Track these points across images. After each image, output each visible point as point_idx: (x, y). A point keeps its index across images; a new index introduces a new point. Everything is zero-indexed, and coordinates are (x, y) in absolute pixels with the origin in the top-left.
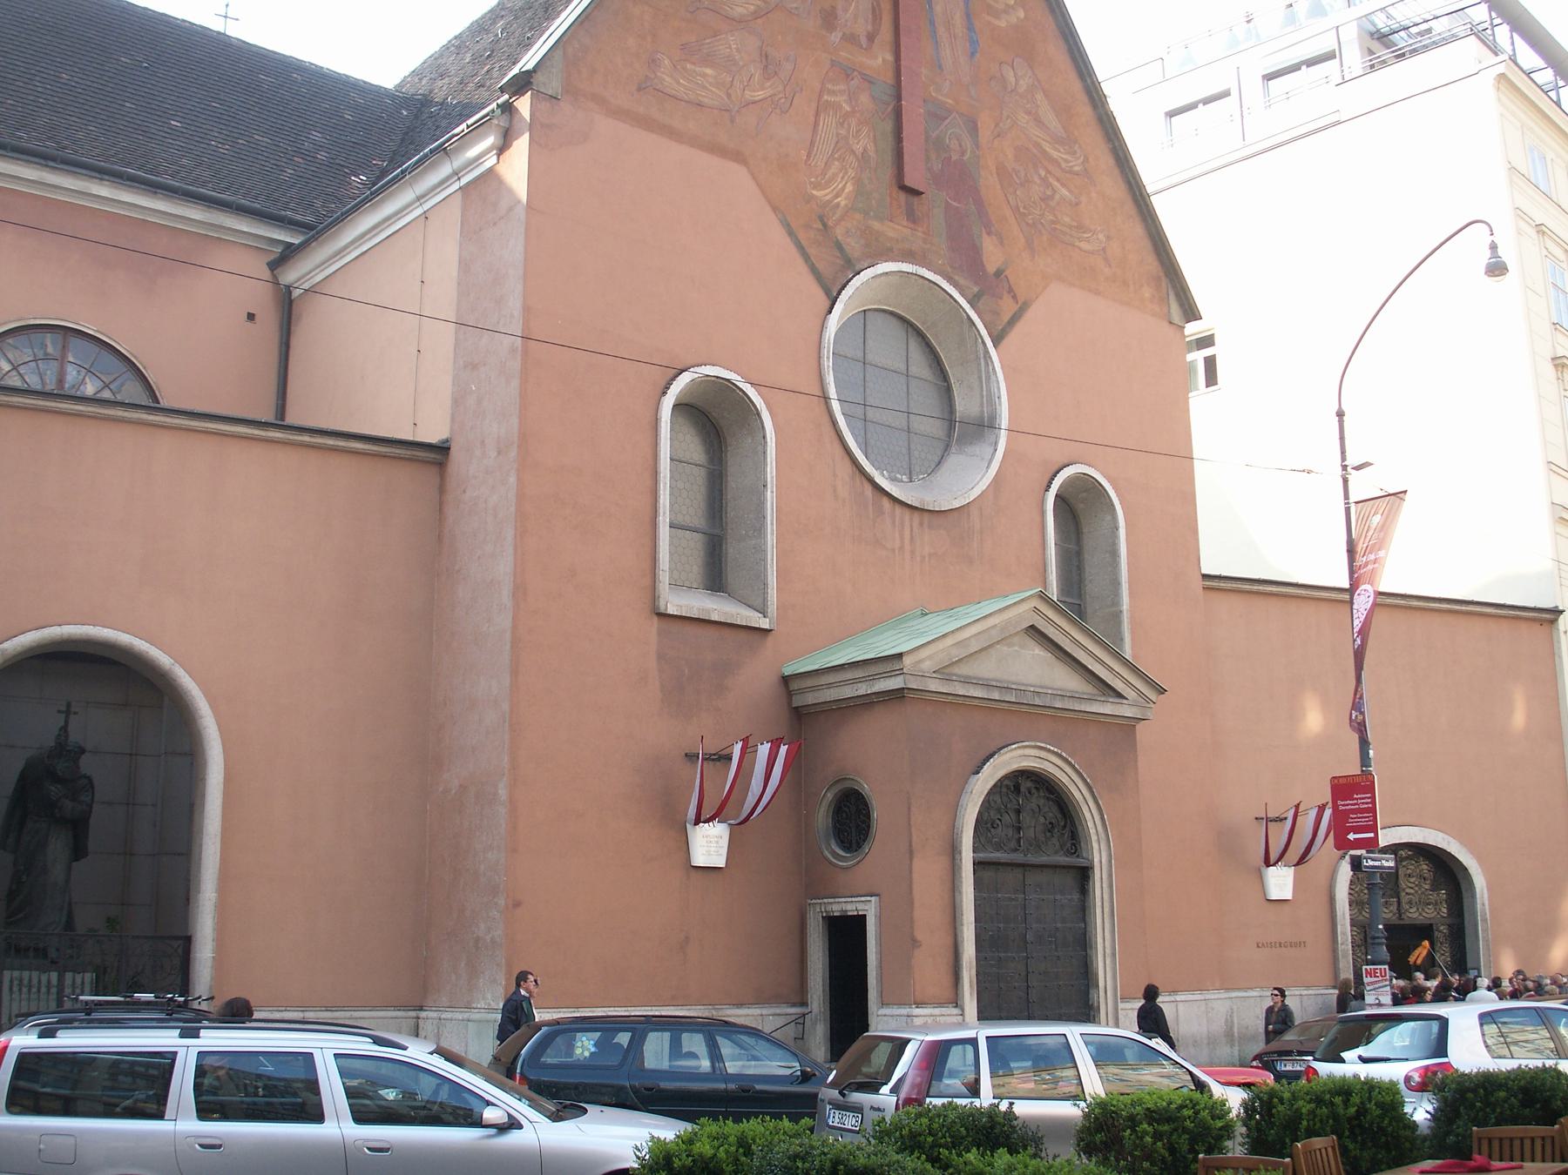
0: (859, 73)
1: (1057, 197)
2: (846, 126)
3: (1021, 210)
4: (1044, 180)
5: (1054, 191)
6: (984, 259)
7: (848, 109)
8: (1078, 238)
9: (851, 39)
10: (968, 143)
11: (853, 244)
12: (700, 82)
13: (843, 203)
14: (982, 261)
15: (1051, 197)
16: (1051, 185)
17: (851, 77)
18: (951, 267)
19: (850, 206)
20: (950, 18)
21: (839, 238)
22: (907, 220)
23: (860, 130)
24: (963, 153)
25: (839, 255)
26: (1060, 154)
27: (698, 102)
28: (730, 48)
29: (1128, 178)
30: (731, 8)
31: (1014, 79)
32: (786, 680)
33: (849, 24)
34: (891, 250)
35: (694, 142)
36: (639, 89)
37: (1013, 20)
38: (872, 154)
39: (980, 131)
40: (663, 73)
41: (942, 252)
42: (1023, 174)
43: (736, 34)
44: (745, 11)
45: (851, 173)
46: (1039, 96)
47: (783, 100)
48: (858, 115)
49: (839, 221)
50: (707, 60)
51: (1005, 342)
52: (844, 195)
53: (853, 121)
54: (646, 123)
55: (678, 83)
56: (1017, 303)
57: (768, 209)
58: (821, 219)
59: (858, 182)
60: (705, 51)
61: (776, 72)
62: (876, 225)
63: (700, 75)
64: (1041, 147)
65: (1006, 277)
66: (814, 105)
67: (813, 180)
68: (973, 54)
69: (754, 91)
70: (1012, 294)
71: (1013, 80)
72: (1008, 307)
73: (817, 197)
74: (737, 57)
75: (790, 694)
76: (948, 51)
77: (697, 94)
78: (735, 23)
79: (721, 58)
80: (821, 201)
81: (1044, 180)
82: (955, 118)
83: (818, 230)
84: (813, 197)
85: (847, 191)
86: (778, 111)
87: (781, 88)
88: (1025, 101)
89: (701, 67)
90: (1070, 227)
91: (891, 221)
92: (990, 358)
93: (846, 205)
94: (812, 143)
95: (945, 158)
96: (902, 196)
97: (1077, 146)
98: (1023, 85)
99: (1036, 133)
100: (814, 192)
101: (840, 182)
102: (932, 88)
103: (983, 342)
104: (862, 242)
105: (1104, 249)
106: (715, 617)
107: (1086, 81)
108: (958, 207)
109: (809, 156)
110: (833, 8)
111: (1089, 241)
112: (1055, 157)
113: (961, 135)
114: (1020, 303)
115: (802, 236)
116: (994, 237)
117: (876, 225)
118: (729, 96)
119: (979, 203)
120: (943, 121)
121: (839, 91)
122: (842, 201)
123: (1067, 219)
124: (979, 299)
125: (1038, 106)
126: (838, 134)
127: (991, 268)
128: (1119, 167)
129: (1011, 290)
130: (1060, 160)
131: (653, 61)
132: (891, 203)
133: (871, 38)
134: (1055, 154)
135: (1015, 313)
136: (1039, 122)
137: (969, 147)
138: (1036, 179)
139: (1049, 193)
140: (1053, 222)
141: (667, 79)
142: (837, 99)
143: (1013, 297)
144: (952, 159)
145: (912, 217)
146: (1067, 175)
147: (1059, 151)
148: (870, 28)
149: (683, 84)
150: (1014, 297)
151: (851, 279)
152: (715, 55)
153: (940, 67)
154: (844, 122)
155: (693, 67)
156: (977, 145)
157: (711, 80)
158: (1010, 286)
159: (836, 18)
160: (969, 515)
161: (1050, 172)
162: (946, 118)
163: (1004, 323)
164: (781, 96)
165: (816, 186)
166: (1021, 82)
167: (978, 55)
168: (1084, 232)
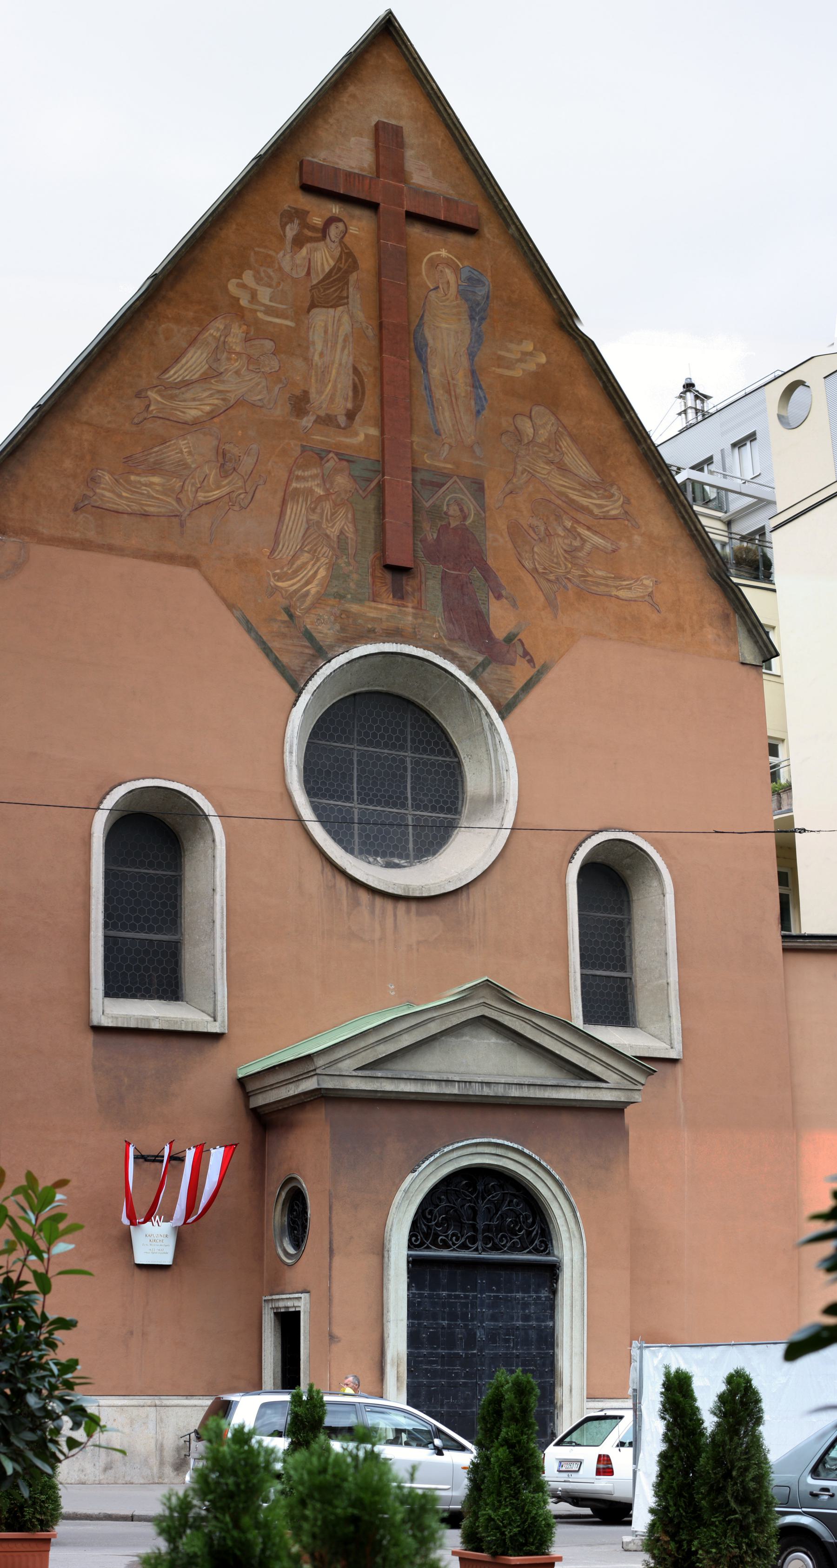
0: (337, 454)
1: (588, 547)
2: (318, 510)
4: (572, 533)
5: (584, 541)
6: (491, 626)
7: (322, 493)
8: (616, 587)
9: (327, 421)
10: (471, 505)
11: (325, 631)
12: (145, 492)
13: (313, 591)
14: (488, 628)
15: (581, 548)
16: (579, 534)
17: (325, 459)
18: (451, 640)
19: (323, 592)
20: (450, 379)
21: (308, 627)
22: (394, 597)
23: (336, 512)
24: (465, 518)
25: (307, 644)
26: (590, 500)
27: (143, 512)
28: (181, 452)
29: (680, 512)
30: (184, 412)
31: (532, 430)
32: (242, 1082)
33: (324, 406)
34: (372, 631)
35: (140, 554)
36: (76, 509)
37: (532, 367)
38: (350, 535)
39: (487, 492)
40: (103, 489)
41: (437, 625)
42: (542, 529)
43: (189, 437)
44: (200, 413)
46: (566, 443)
47: (242, 496)
48: (333, 497)
49: (308, 610)
50: (155, 469)
51: (517, 712)
52: (316, 582)
53: (327, 506)
55: (120, 496)
56: (534, 667)
57: (223, 608)
58: (289, 612)
59: (333, 567)
60: (152, 460)
61: (234, 469)
62: (355, 608)
63: (145, 485)
64: (567, 497)
65: (520, 640)
66: (280, 495)
67: (278, 571)
68: (478, 412)
69: (208, 492)
70: (528, 658)
71: (530, 431)
72: (521, 672)
73: (282, 588)
74: (188, 461)
75: (247, 1096)
76: (447, 414)
77: (143, 504)
78: (186, 426)
79: (170, 464)
80: (286, 591)
81: (572, 533)
82: (455, 482)
83: (284, 622)
84: (277, 588)
85: (319, 576)
86: (237, 508)
87: (240, 483)
88: (546, 451)
89: (146, 477)
90: (605, 578)
91: (374, 601)
92: (496, 729)
93: (318, 592)
94: (277, 534)
95: (441, 526)
96: (388, 576)
97: (615, 487)
98: (544, 434)
99: (561, 482)
100: (279, 584)
101: (311, 569)
102: (426, 455)
103: (487, 714)
104: (337, 627)
105: (650, 595)
106: (156, 1025)
107: (624, 417)
108: (457, 576)
109: (273, 551)
110: (306, 393)
111: (630, 589)
112: (585, 504)
113: (462, 499)
114: (538, 667)
115: (263, 632)
116: (505, 600)
117: (355, 608)
118: (179, 500)
120: (440, 488)
121: (311, 476)
122: (313, 588)
124: (484, 669)
125: (563, 453)
126: (308, 521)
127: (499, 633)
128: (671, 502)
129: (526, 653)
130: (591, 507)
131: (93, 479)
132: (374, 582)
133: (351, 416)
134: (584, 501)
135: (531, 678)
136: (563, 469)
137: (472, 507)
138: (560, 532)
139: (577, 543)
141: (107, 494)
142: (308, 484)
144: (451, 527)
145: (399, 594)
146: (602, 521)
147: (591, 497)
148: (350, 405)
149: (127, 498)
150: (531, 661)
151: (321, 668)
152: (161, 463)
153: (438, 433)
154: (315, 508)
155: (138, 478)
156: (483, 507)
157: (158, 488)
158: (525, 650)
159: (308, 402)
160: (468, 898)
161: (578, 522)
162: (444, 485)
163: (516, 691)
164: (241, 491)
165: (280, 578)
166: (541, 431)
167: (485, 413)
168: (624, 580)
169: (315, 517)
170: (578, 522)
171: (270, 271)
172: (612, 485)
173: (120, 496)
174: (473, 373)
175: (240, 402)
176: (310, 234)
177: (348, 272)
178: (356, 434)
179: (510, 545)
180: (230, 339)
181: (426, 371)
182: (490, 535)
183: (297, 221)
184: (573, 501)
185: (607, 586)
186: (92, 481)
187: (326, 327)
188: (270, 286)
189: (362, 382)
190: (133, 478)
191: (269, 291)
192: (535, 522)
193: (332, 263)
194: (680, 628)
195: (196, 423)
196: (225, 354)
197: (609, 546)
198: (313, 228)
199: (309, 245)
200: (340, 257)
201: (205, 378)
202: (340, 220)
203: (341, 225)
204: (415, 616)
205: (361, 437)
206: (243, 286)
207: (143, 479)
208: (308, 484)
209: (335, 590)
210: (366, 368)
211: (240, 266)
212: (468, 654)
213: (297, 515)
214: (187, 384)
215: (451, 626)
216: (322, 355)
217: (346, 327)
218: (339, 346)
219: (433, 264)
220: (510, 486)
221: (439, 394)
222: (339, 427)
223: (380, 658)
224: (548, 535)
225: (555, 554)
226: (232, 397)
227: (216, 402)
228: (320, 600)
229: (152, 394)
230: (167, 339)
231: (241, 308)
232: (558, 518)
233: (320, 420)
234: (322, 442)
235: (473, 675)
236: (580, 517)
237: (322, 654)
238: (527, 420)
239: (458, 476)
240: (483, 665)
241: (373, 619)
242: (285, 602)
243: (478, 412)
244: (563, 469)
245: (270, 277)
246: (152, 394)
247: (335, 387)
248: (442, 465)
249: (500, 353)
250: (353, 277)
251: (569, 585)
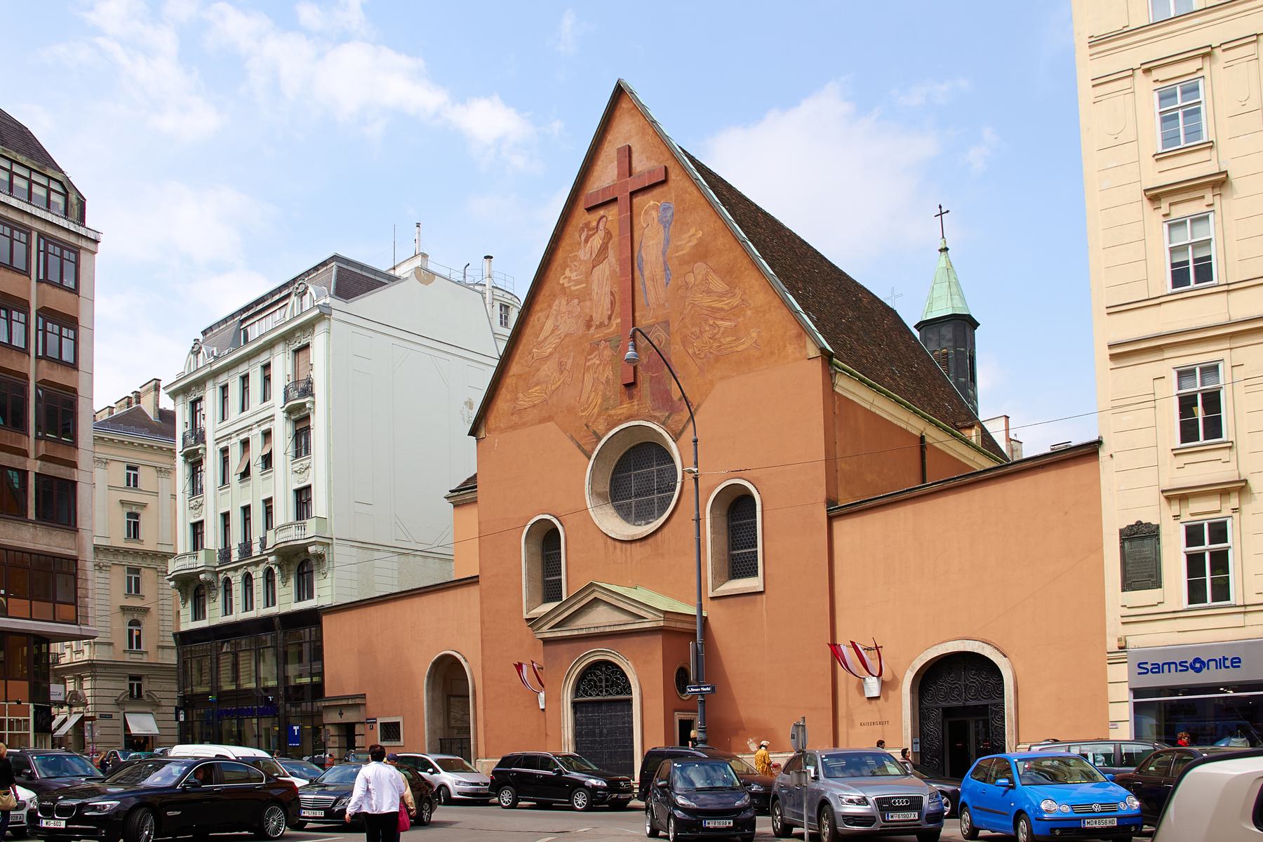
3: (697, 352)
4: (714, 326)
5: (719, 327)
9: (601, 325)
10: (663, 335)
34: (620, 420)
37: (694, 242)
45: (600, 393)
49: (594, 422)
54: (514, 427)
59: (604, 395)
62: (612, 412)
68: (667, 283)
76: (652, 293)
90: (730, 343)
91: (621, 405)
104: (606, 424)
110: (591, 316)
117: (612, 412)
122: (596, 410)
123: (728, 339)
130: (724, 306)
133: (610, 318)
134: (720, 305)
136: (709, 292)
140: (720, 346)
141: (521, 402)
145: (631, 397)
147: (724, 301)
148: (609, 313)
153: (648, 305)
165: (583, 411)
169: (596, 376)
170: (716, 318)
171: (576, 263)
172: (735, 289)
173: (525, 402)
174: (665, 262)
175: (566, 336)
176: (591, 233)
177: (608, 243)
178: (612, 325)
179: (682, 348)
180: (561, 307)
181: (642, 275)
182: (672, 347)
183: (586, 230)
184: (713, 308)
185: (731, 347)
186: (517, 399)
187: (599, 279)
188: (576, 271)
189: (614, 298)
190: (530, 391)
191: (575, 273)
192: (694, 330)
193: (601, 242)
194: (772, 353)
195: (551, 354)
196: (560, 316)
197: (733, 324)
198: (593, 229)
199: (591, 239)
200: (604, 239)
201: (553, 332)
202: (604, 216)
203: (604, 219)
204: (638, 405)
205: (615, 325)
206: (565, 278)
207: (533, 390)
208: (594, 360)
209: (605, 407)
210: (616, 289)
211: (565, 266)
212: (661, 414)
213: (589, 378)
214: (546, 338)
215: (654, 403)
216: (597, 294)
217: (607, 272)
218: (604, 285)
219: (646, 212)
220: (682, 316)
221: (649, 284)
222: (605, 326)
223: (623, 432)
224: (701, 333)
226: (562, 335)
227: (557, 341)
228: (599, 415)
229: (534, 350)
230: (538, 321)
231: (565, 288)
232: (706, 321)
233: (598, 327)
234: (599, 337)
235: (664, 424)
236: (718, 315)
237: (599, 439)
238: (692, 274)
239: (658, 324)
240: (668, 417)
241: (621, 414)
242: (585, 421)
243: (667, 283)
244: (709, 292)
245: (576, 266)
246: (534, 350)
247: (603, 308)
248: (650, 321)
249: (678, 244)
250: (609, 245)
251: (711, 356)
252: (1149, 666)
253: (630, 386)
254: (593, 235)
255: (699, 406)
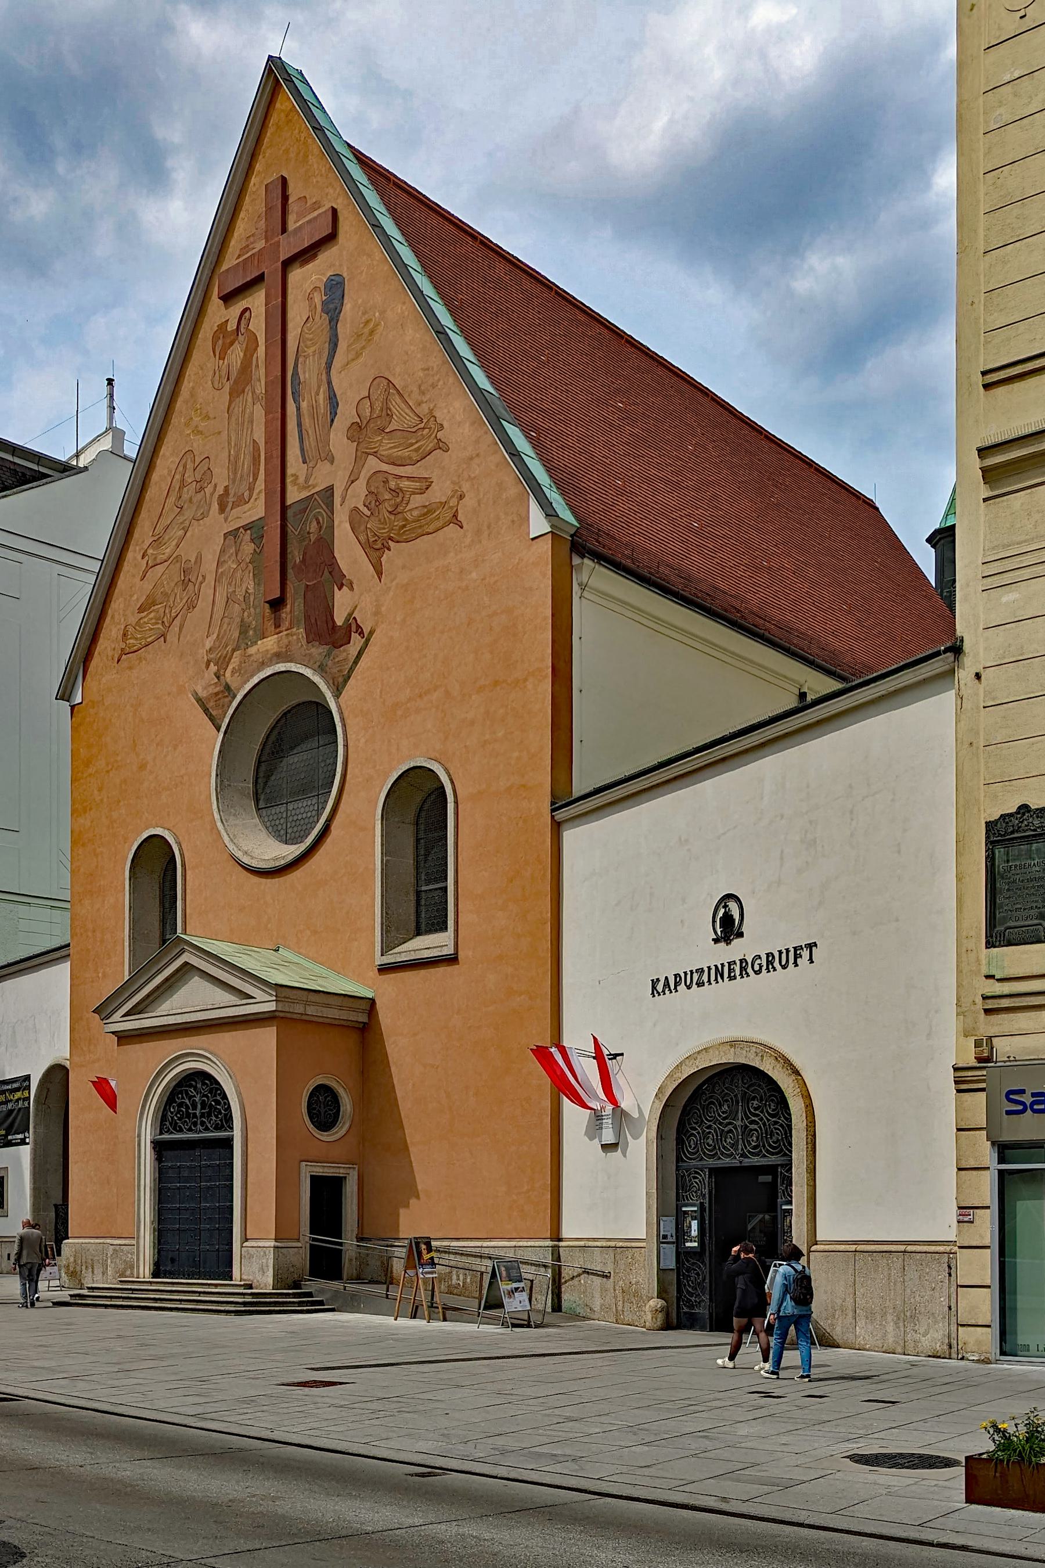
2: (234, 583)
30: (164, 554)
56: (364, 637)
119: (332, 565)
127: (339, 621)
138: (387, 496)
140: (404, 526)
143: (359, 635)
150: (361, 633)
185: (420, 527)
203: (247, 314)
225: (382, 520)
252: (1027, 1099)
253: (277, 604)
254: (232, 343)
255: (371, 633)
